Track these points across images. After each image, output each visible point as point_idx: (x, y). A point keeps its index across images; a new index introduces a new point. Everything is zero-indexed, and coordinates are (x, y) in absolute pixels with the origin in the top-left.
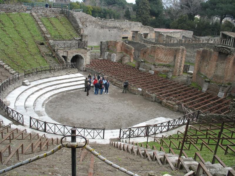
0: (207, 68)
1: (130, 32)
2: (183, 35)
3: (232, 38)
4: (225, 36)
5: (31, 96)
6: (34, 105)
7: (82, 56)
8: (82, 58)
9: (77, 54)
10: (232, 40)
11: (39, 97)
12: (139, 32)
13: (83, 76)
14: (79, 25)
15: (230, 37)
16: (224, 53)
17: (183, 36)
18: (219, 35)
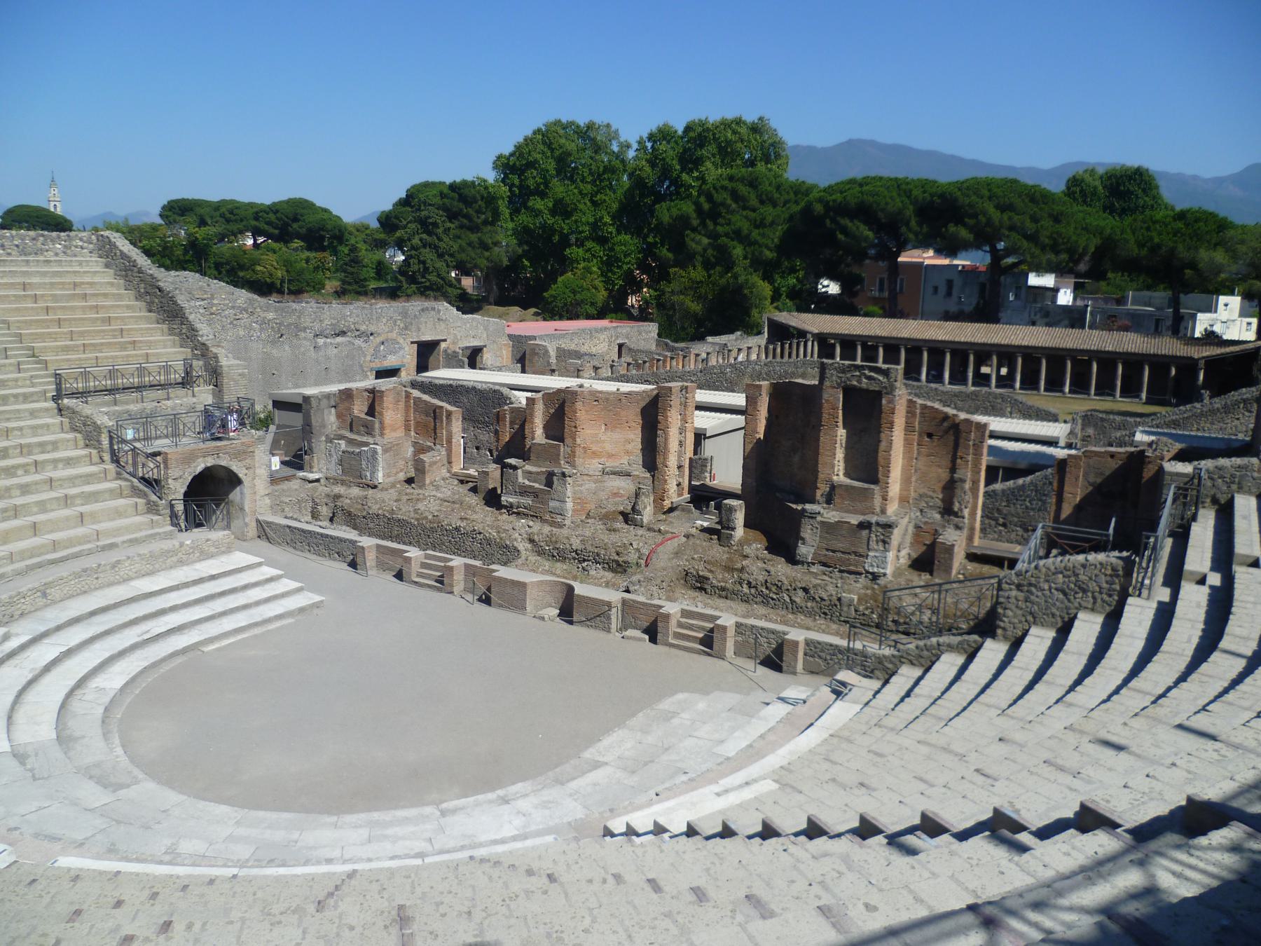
0: (796, 459)
1: (405, 345)
2: (620, 341)
3: (809, 336)
4: (781, 333)
5: (30, 696)
6: (64, 739)
7: (234, 468)
8: (235, 481)
9: (210, 462)
10: (810, 344)
11: (70, 695)
12: (443, 345)
13: (260, 564)
14: (198, 326)
15: (802, 334)
16: (867, 391)
17: (620, 346)
18: (751, 329)
